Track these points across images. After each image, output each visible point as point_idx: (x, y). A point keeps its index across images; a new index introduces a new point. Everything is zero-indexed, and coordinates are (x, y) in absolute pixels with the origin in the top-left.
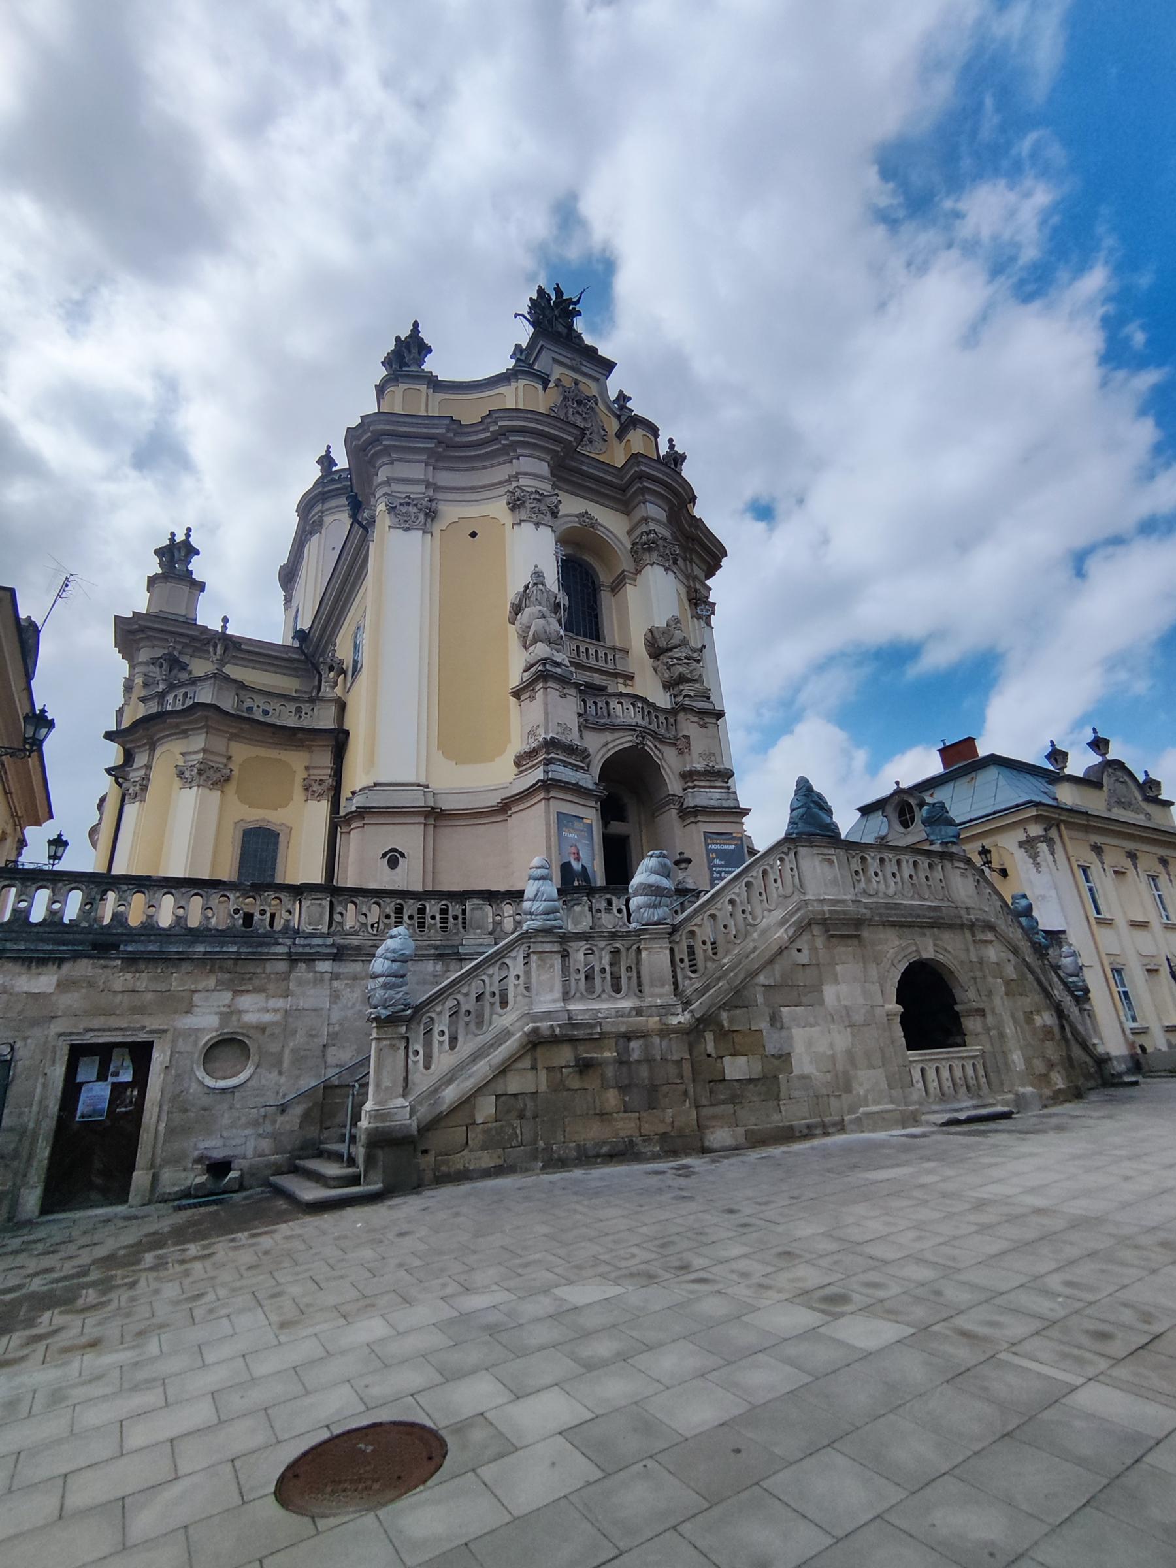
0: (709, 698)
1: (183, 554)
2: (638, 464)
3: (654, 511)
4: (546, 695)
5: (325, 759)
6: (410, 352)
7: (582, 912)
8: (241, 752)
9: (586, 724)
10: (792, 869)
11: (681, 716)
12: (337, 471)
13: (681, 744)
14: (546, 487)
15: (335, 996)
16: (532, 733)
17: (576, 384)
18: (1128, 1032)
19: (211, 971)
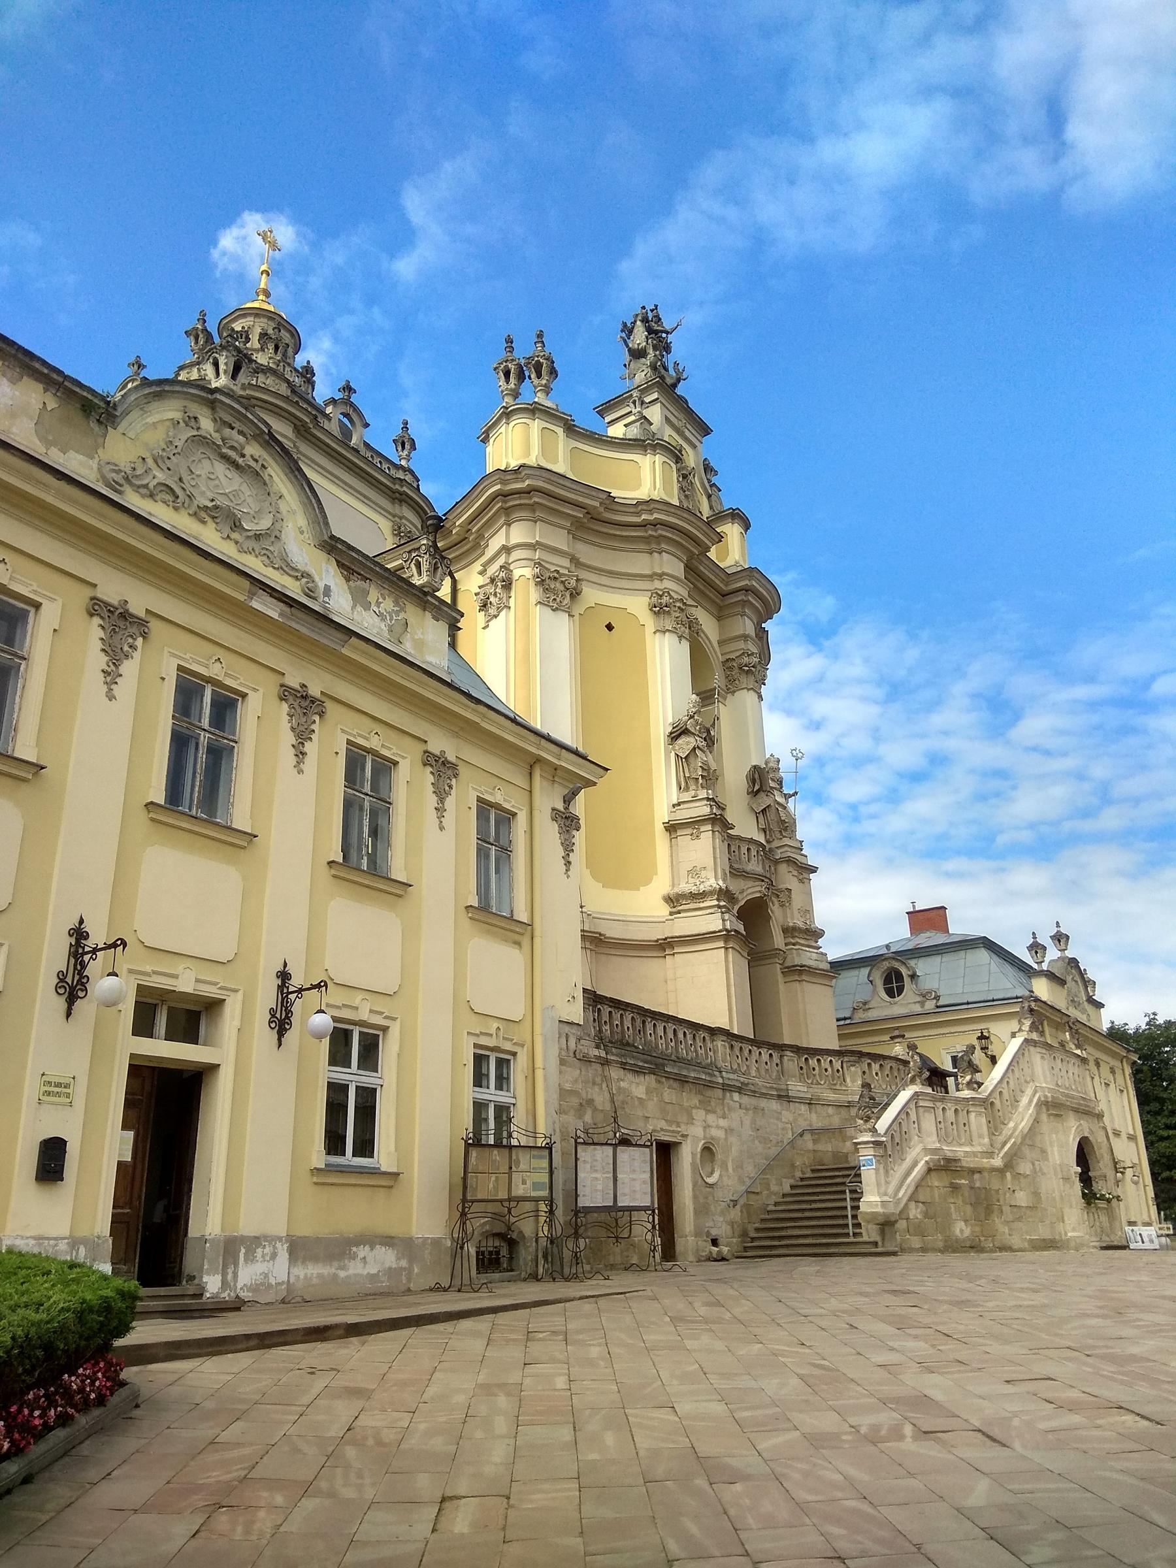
2: (751, 578)
3: (750, 629)
7: (856, 1072)
16: (693, 872)
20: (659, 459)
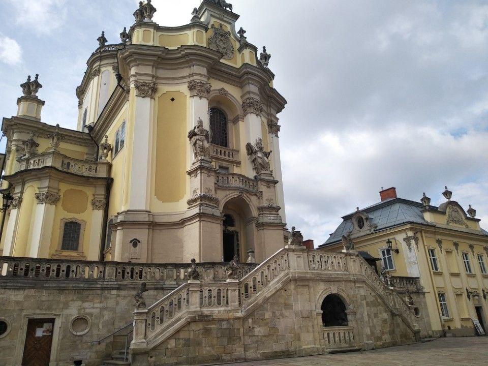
0: (272, 175)
1: (34, 87)
2: (246, 68)
3: (253, 88)
4: (201, 176)
5: (102, 191)
6: (146, 12)
8: (64, 187)
9: (218, 187)
10: (286, 260)
11: (259, 183)
12: (108, 46)
13: (259, 195)
14: (205, 80)
15: (117, 303)
16: (195, 191)
17: (221, 26)
18: (443, 321)
19: (75, 294)
20: (196, 30)
